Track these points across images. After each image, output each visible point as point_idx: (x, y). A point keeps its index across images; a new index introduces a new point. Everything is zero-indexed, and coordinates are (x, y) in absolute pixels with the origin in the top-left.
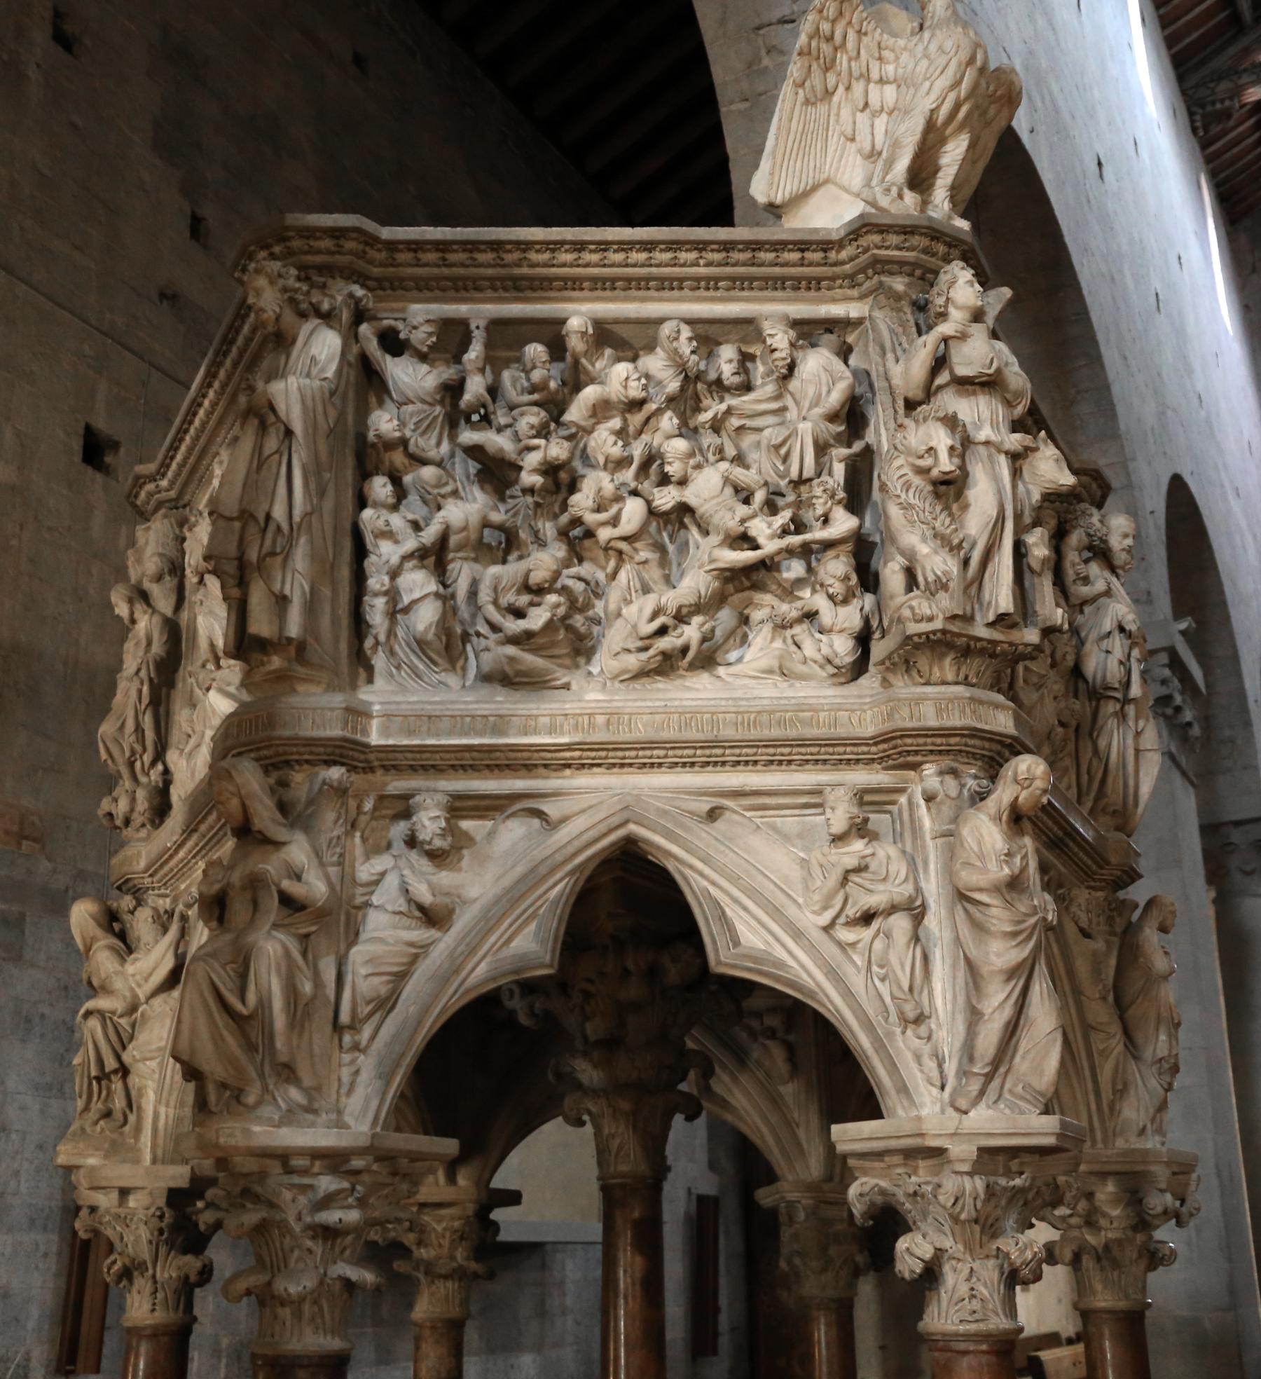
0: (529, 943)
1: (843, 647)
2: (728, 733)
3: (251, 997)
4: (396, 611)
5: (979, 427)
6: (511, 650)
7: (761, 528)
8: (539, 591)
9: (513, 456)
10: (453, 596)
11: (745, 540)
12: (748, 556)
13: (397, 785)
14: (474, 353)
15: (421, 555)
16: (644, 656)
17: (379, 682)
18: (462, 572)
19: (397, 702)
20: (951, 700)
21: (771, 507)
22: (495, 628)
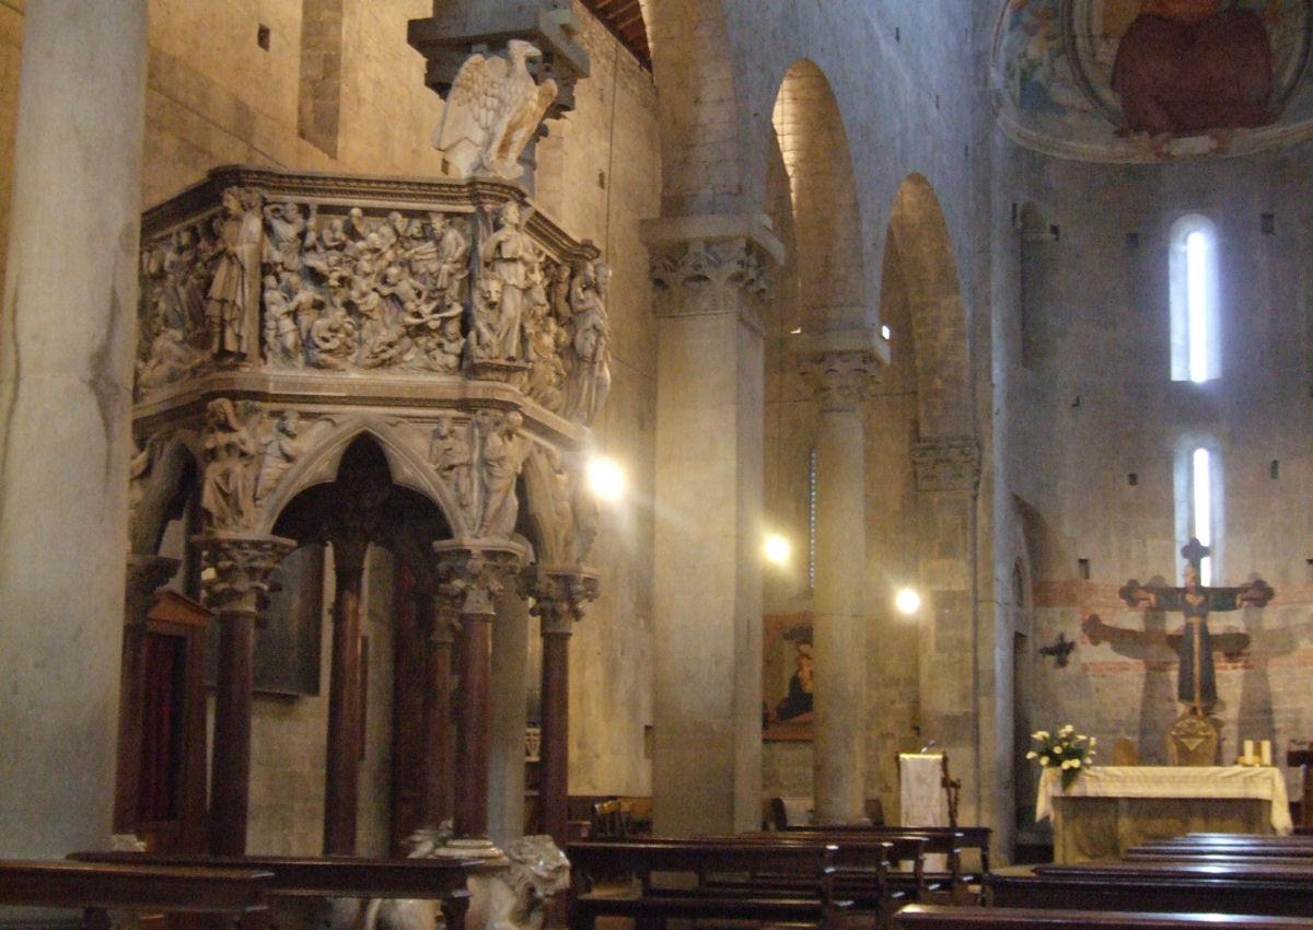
0: (324, 468)
1: (452, 360)
2: (406, 395)
3: (231, 487)
4: (278, 336)
5: (510, 278)
6: (324, 356)
7: (426, 309)
8: (336, 331)
9: (327, 273)
10: (299, 329)
11: (417, 315)
12: (418, 321)
13: (276, 407)
14: (312, 222)
15: (288, 313)
16: (374, 361)
17: (270, 364)
18: (304, 319)
19: (275, 374)
20: (489, 388)
21: (429, 299)
22: (317, 346)
